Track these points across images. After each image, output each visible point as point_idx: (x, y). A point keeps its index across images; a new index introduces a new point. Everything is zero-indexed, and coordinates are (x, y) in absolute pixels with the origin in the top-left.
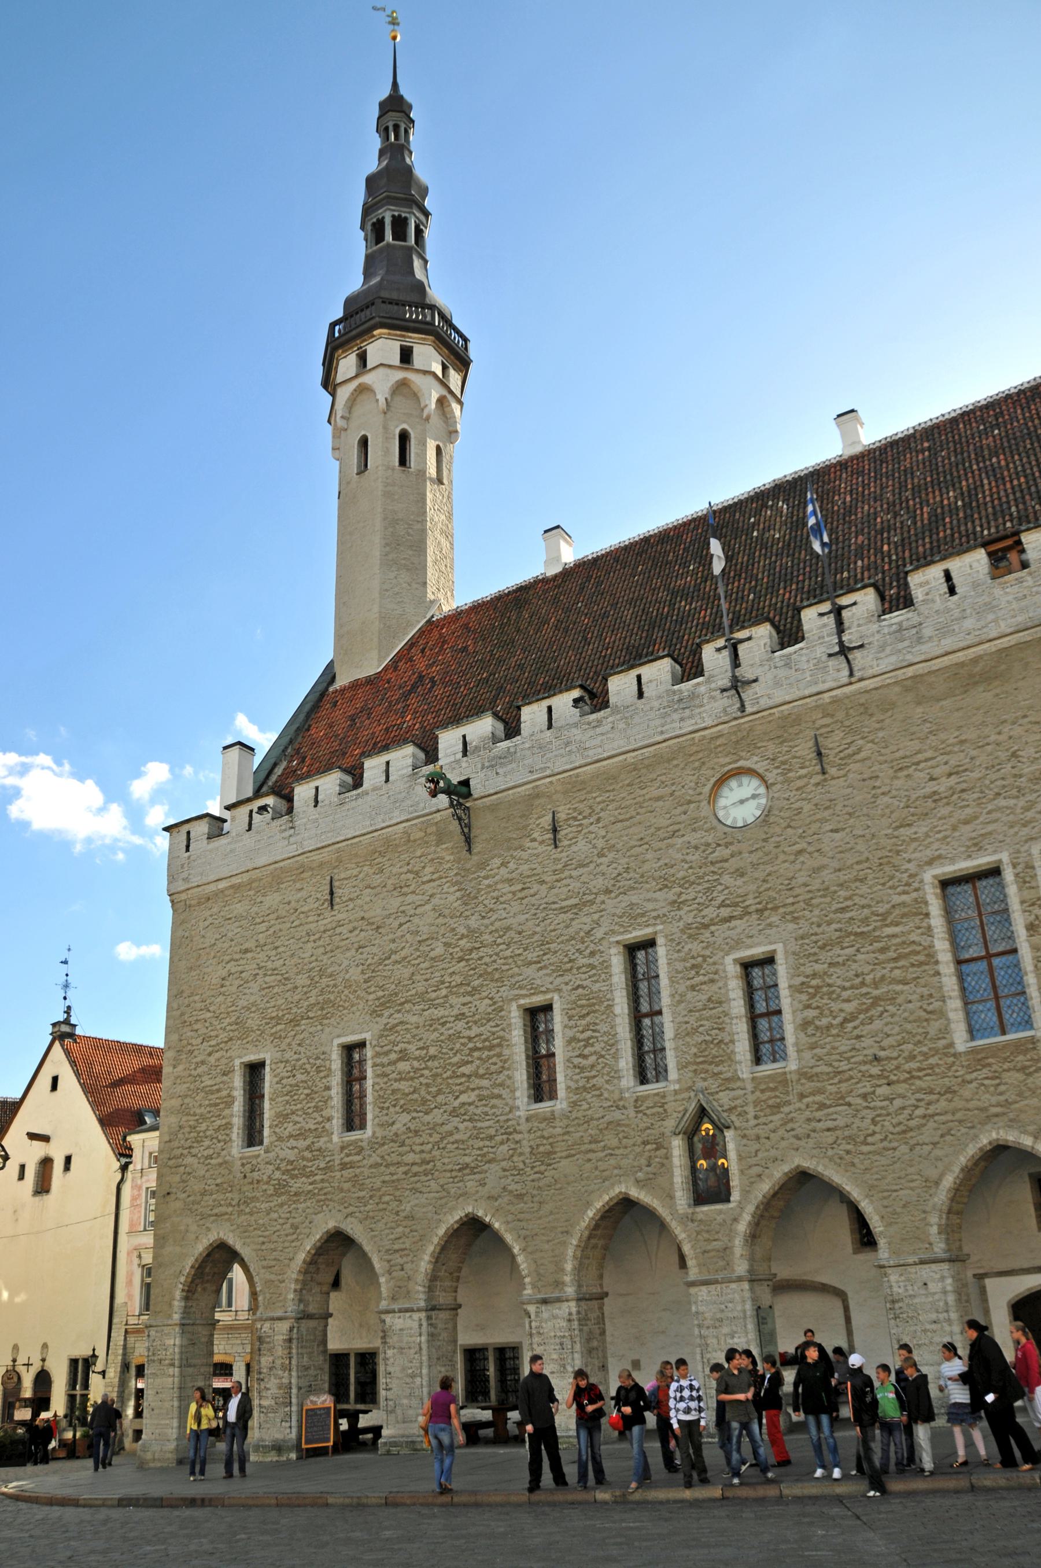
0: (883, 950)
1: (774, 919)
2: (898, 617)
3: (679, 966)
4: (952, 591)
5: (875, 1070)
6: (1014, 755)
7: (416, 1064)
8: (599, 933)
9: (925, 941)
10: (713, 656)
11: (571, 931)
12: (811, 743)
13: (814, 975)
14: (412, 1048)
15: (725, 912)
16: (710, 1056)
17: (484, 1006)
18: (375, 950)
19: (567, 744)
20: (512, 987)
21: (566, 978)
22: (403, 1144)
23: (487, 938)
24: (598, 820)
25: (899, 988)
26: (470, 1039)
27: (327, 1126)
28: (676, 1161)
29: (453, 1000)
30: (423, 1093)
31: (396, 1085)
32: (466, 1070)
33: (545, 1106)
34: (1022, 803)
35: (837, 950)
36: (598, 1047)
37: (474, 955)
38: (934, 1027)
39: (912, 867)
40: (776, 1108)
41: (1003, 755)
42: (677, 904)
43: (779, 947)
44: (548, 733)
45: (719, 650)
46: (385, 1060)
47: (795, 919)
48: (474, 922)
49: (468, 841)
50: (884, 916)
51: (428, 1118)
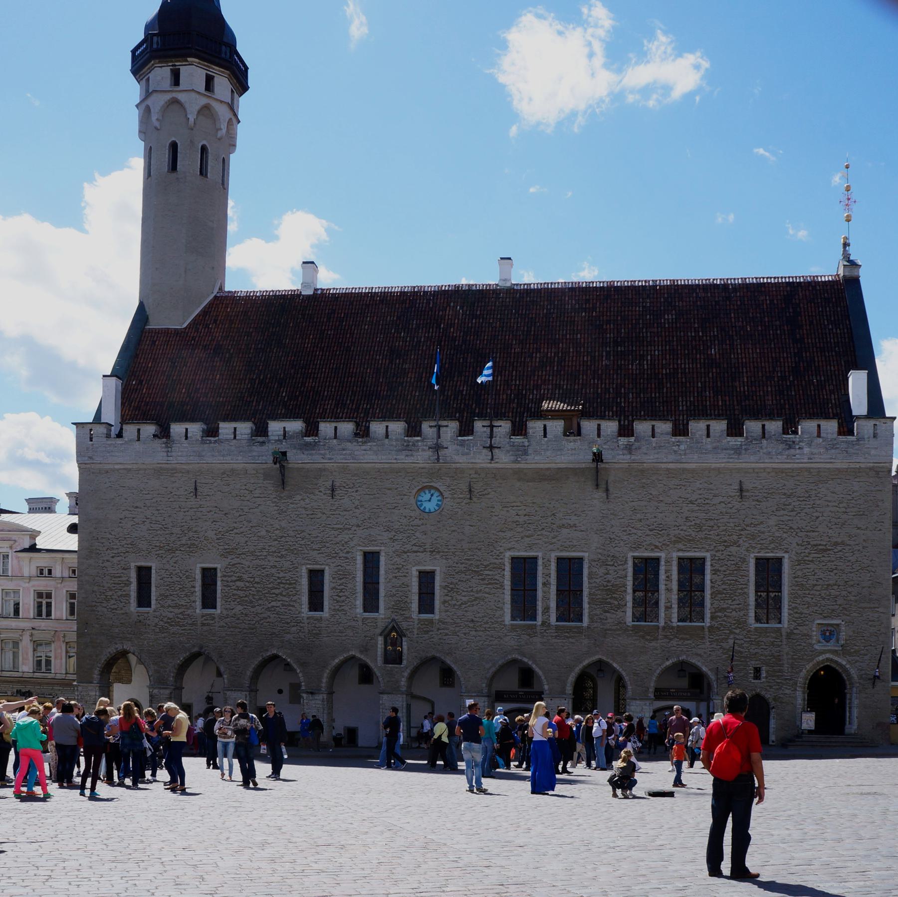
0: (483, 579)
1: (438, 556)
2: (518, 439)
3: (391, 567)
4: (545, 436)
5: (471, 625)
6: (553, 514)
7: (247, 584)
8: (352, 544)
9: (501, 580)
10: (427, 428)
11: (338, 540)
12: (467, 484)
13: (452, 583)
14: (245, 577)
15: (415, 548)
16: (400, 606)
17: (287, 564)
18: (223, 524)
19: (344, 450)
20: (303, 558)
21: (333, 560)
22: (238, 619)
23: (292, 533)
24: (357, 491)
25: (487, 595)
26: (279, 578)
27: (193, 604)
28: (379, 646)
29: (269, 558)
30: (251, 597)
31: (235, 592)
32: (277, 591)
33: (317, 614)
34: (552, 535)
35: (463, 575)
36: (346, 593)
37: (283, 539)
38: (498, 614)
39: (502, 550)
40: (427, 632)
41: (549, 514)
42: (393, 540)
43: (438, 569)
44: (335, 441)
45: (431, 427)
46: (229, 579)
47: (447, 559)
48: (283, 524)
49: (283, 483)
50: (486, 566)
51: (252, 610)
